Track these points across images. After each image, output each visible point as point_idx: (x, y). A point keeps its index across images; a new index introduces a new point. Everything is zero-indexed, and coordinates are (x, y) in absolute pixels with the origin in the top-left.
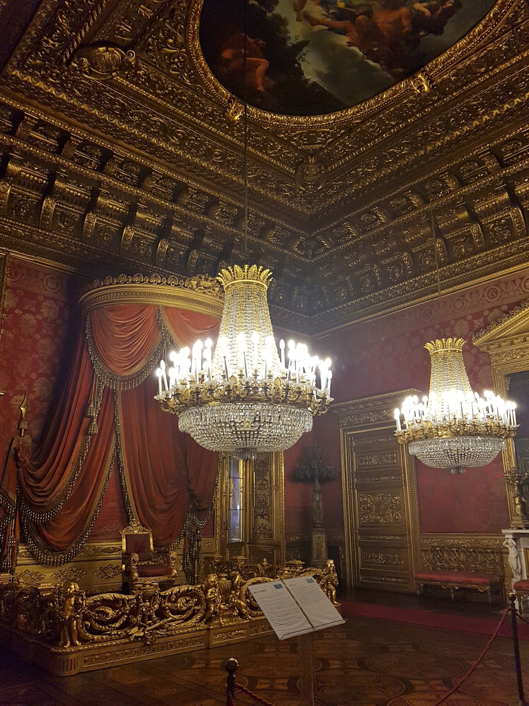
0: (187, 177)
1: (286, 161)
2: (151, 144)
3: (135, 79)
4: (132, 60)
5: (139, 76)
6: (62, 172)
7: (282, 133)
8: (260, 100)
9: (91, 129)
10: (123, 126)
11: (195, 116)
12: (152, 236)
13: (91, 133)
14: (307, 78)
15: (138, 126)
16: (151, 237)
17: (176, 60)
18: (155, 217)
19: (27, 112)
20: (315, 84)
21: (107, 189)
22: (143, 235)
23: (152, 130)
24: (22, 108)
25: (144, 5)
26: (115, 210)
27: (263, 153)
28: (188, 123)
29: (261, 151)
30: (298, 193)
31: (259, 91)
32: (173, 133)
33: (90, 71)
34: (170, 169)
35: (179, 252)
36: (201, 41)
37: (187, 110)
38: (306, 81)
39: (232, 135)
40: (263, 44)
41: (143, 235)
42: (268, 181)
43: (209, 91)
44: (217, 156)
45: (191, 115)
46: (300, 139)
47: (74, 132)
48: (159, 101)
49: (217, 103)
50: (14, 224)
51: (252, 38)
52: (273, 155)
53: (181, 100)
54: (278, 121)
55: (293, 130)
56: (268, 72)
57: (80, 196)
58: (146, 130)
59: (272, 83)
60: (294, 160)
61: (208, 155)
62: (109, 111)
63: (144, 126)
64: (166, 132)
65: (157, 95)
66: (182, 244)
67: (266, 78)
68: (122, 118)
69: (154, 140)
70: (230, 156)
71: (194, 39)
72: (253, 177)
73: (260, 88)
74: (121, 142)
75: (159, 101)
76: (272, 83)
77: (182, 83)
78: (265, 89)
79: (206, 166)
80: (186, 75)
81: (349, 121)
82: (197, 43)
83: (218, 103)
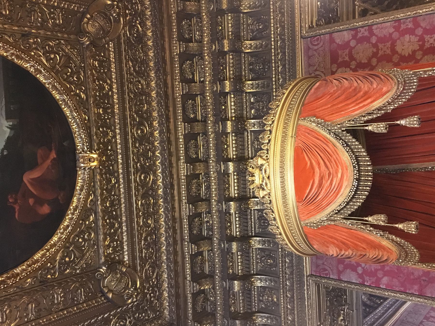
0: (177, 139)
1: (104, 63)
2: (165, 192)
3: (118, 249)
4: (103, 269)
5: (114, 249)
6: (224, 246)
7: (80, 96)
8: (65, 144)
9: (179, 242)
10: (163, 223)
11: (118, 181)
12: (248, 136)
13: (182, 239)
14: (9, 130)
15: (156, 212)
16: (249, 137)
17: (80, 240)
18: (228, 146)
19: (190, 291)
20: (8, 118)
21: (222, 204)
22: (250, 146)
23: (152, 201)
24: (189, 295)
25: (54, 302)
26: (238, 182)
27: (113, 92)
28: (128, 182)
29: (112, 96)
30: (130, 14)
31: (57, 154)
32: (144, 184)
33: (132, 287)
34: (178, 159)
35: (252, 103)
36: (50, 237)
37: (117, 191)
38: (11, 128)
39: (114, 137)
40: (12, 197)
41: (250, 146)
42: (137, 61)
43: (88, 195)
44: (142, 131)
45: (119, 185)
46: (72, 75)
47: (188, 252)
48: (124, 219)
49: (94, 179)
50: (282, 271)
51: (14, 209)
52: (109, 81)
53: (112, 205)
54: (71, 111)
55: (68, 91)
56: (34, 165)
57: (239, 217)
58: (156, 204)
59: (40, 152)
60: (99, 55)
61: (146, 139)
62: (156, 243)
63: (153, 209)
64: (148, 192)
65: (120, 224)
66: (242, 103)
67: (39, 160)
68: (157, 229)
69: (160, 192)
70: (134, 120)
71: (52, 246)
72: (142, 78)
73: (53, 155)
74: (177, 215)
75: (124, 219)
76: (40, 152)
77: (96, 221)
78: (51, 150)
79: (157, 132)
80: (87, 223)
81: (14, 46)
82: (55, 239)
83: (92, 178)
